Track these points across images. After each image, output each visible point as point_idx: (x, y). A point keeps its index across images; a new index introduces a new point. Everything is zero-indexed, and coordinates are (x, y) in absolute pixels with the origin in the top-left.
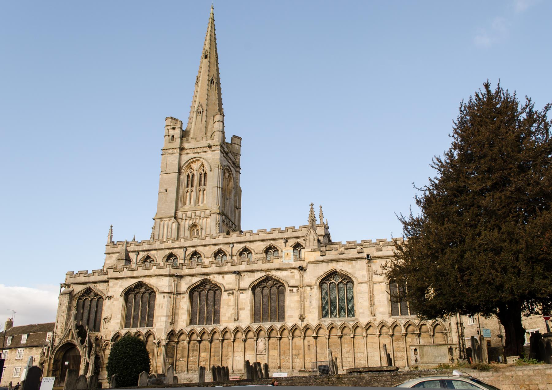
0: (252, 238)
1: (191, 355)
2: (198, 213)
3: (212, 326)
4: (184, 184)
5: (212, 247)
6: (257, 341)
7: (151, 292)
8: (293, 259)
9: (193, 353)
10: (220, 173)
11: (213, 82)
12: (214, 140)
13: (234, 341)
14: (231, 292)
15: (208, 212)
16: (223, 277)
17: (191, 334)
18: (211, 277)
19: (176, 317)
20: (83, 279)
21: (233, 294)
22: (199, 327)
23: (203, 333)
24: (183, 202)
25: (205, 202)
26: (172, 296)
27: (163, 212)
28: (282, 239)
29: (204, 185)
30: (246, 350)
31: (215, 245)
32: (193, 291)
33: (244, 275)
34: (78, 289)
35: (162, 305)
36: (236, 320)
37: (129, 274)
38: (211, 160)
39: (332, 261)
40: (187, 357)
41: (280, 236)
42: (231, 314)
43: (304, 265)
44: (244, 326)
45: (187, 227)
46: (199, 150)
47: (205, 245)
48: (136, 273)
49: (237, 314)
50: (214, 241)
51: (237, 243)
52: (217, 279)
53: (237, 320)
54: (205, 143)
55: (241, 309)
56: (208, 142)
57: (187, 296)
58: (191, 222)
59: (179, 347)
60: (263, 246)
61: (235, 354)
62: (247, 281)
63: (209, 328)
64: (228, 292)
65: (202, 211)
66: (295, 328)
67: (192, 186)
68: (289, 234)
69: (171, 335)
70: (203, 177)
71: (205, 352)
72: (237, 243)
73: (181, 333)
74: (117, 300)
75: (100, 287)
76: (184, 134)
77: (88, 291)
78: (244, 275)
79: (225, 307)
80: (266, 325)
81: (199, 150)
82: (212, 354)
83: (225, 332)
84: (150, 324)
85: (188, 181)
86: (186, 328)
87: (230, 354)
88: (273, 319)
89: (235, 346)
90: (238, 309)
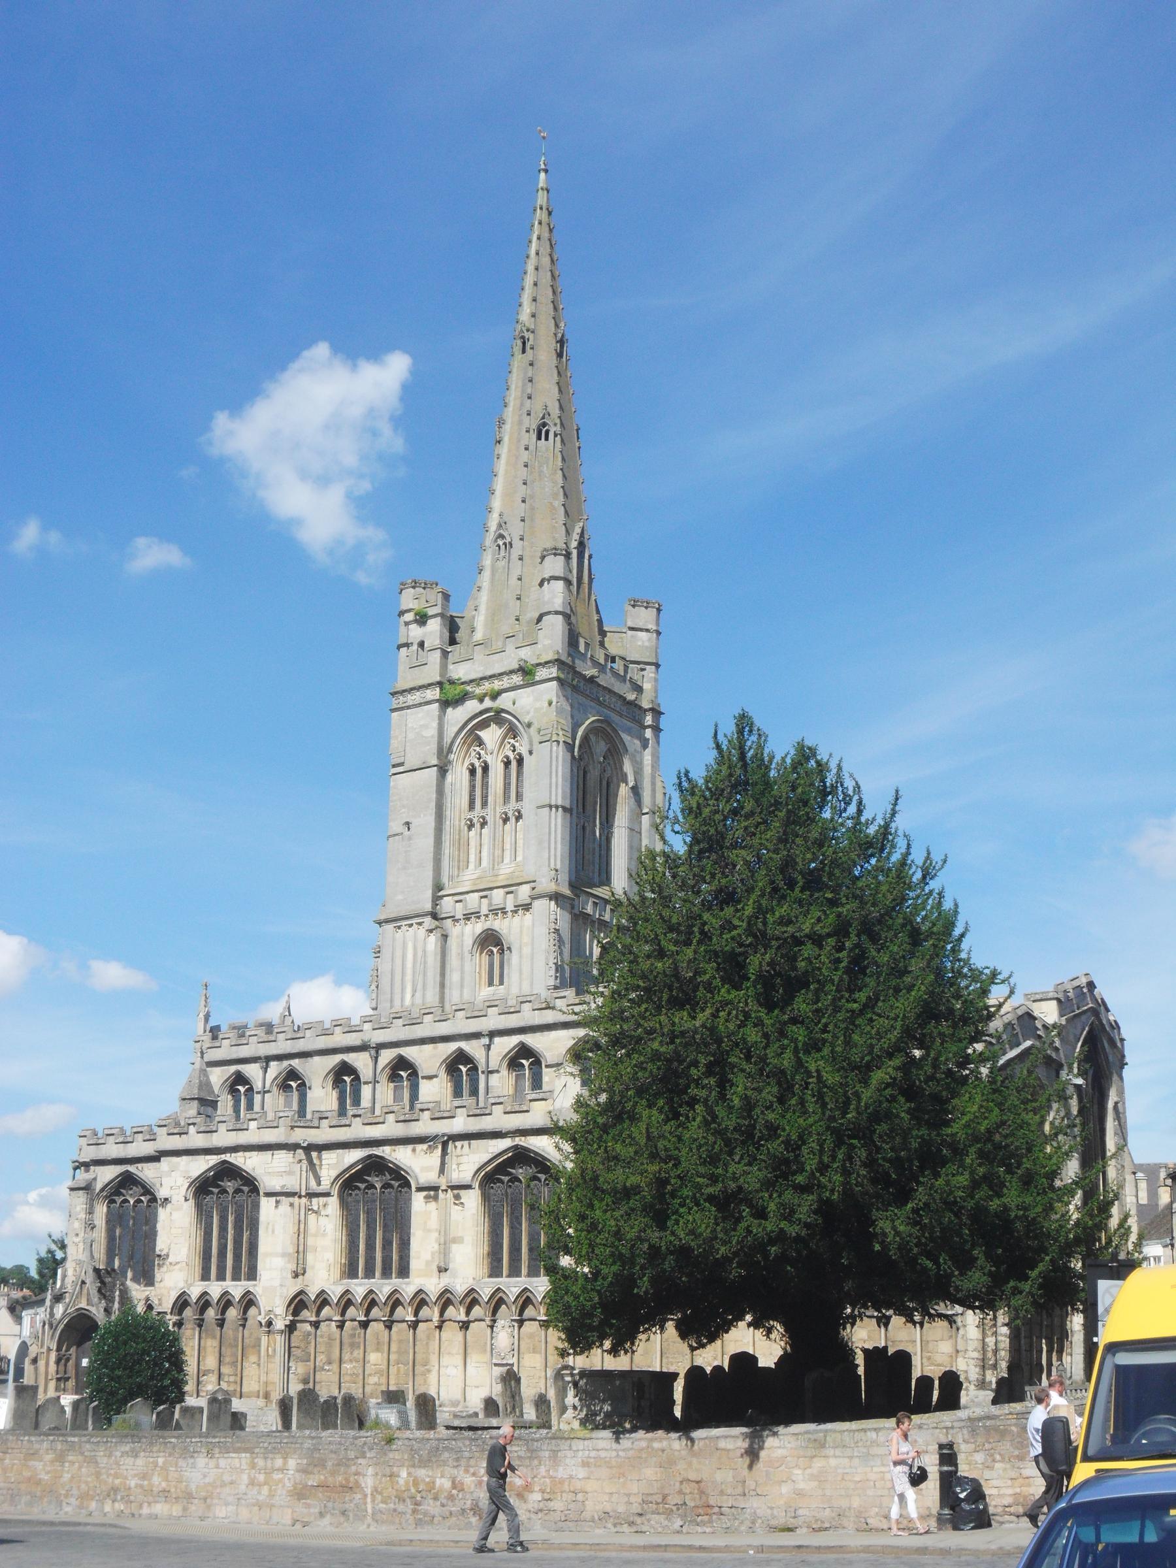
1: (346, 1357)
3: (389, 1284)
4: (458, 801)
5: (441, 1046)
6: (492, 1327)
9: (351, 1353)
10: (557, 757)
11: (547, 432)
12: (539, 646)
13: (440, 1327)
14: (432, 1193)
15: (524, 892)
16: (414, 1150)
17: (346, 1302)
18: (385, 1152)
19: (310, 1258)
20: (112, 1150)
21: (436, 1198)
22: (361, 1285)
23: (371, 1302)
24: (459, 861)
25: (519, 859)
26: (296, 1200)
27: (400, 897)
29: (517, 801)
30: (469, 1350)
33: (462, 1146)
34: (106, 1174)
35: (273, 1226)
36: (442, 1270)
37: (199, 1141)
38: (532, 714)
40: (338, 1362)
42: (433, 1254)
44: (460, 1288)
45: (469, 941)
46: (497, 685)
47: (423, 1041)
50: (444, 1029)
52: (401, 1156)
53: (446, 1270)
54: (510, 660)
55: (456, 1240)
58: (478, 927)
59: (322, 1336)
61: (445, 1360)
63: (383, 1288)
64: (424, 1193)
65: (509, 888)
67: (484, 804)
69: (298, 1304)
71: (378, 1350)
73: (323, 1300)
75: (146, 1172)
77: (127, 1181)
78: (462, 1146)
82: (393, 1357)
83: (420, 1300)
84: (252, 1275)
85: (472, 788)
86: (333, 1287)
87: (434, 1359)
89: (443, 1339)
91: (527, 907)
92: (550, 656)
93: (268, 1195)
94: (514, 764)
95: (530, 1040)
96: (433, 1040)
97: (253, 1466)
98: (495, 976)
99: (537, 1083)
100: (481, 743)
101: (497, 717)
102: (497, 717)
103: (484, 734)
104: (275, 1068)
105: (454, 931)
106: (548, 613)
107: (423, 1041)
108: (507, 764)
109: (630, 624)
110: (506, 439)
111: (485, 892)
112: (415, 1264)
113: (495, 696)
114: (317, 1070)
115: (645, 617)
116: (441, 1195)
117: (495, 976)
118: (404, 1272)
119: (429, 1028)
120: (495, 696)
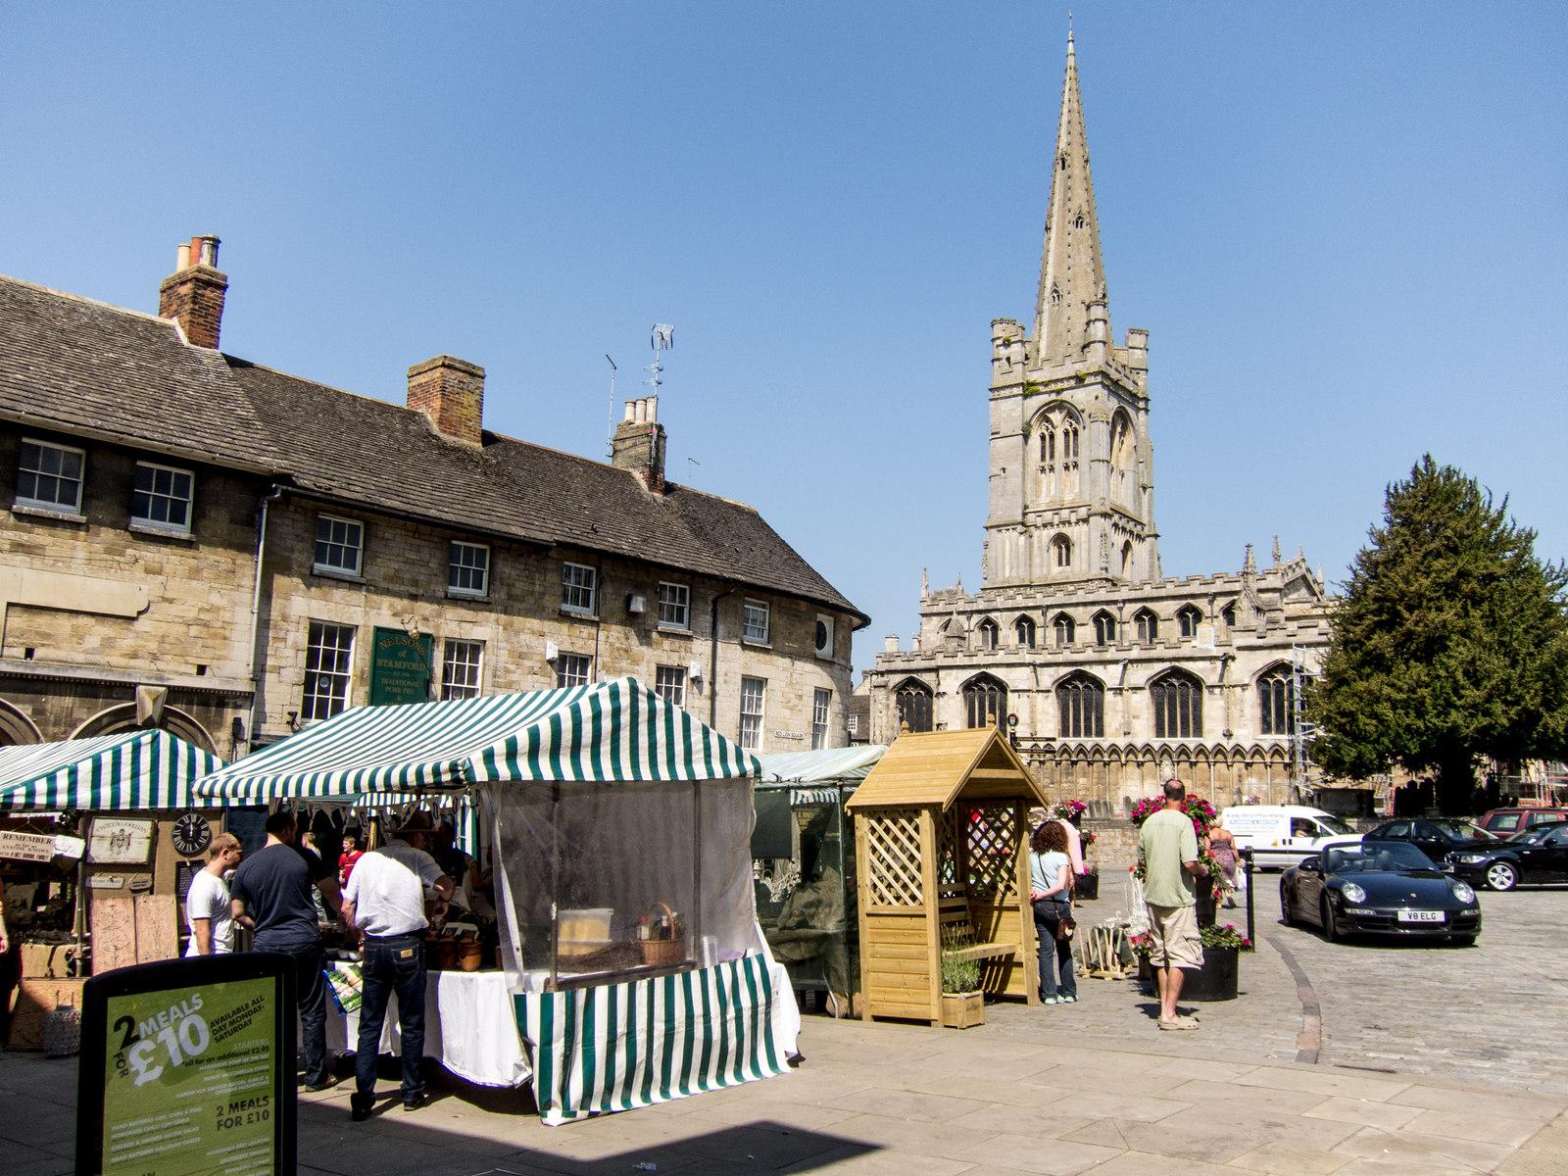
0: (1155, 593)
1: (1064, 780)
2: (1065, 514)
5: (1089, 608)
8: (1213, 643)
12: (1089, 362)
18: (1086, 668)
20: (899, 665)
21: (1121, 694)
28: (1206, 595)
31: (1093, 603)
32: (1062, 685)
34: (898, 678)
36: (1127, 734)
37: (966, 661)
39: (1276, 647)
41: (1204, 589)
43: (1232, 651)
44: (1139, 744)
46: (1060, 386)
47: (1077, 605)
48: (975, 661)
49: (1128, 724)
50: (1091, 598)
51: (1130, 601)
52: (1096, 671)
56: (1078, 366)
57: (1053, 695)
58: (1052, 532)
60: (1174, 606)
63: (1089, 742)
65: (1073, 509)
66: (1219, 750)
67: (1052, 457)
68: (1219, 586)
72: (1130, 601)
74: (953, 698)
75: (927, 678)
77: (911, 682)
79: (1110, 713)
80: (1174, 743)
81: (1060, 386)
83: (1114, 750)
85: (1043, 448)
88: (1185, 734)
90: (1130, 716)
91: (1086, 521)
92: (1095, 369)
93: (1013, 691)
94: (1071, 434)
95: (1149, 605)
96: (1085, 604)
97: (1124, 835)
98: (1065, 559)
99: (1154, 633)
100: (1048, 420)
101: (1060, 405)
102: (1060, 405)
103: (1051, 416)
104: (976, 618)
105: (1036, 533)
106: (1094, 342)
107: (1077, 605)
108: (1066, 434)
109: (1130, 345)
110: (1054, 227)
111: (1056, 511)
112: (1107, 730)
113: (1058, 392)
114: (1005, 621)
115: (1138, 340)
116: (1124, 692)
117: (1065, 559)
118: (1100, 733)
119: (1081, 597)
120: (1058, 392)
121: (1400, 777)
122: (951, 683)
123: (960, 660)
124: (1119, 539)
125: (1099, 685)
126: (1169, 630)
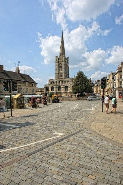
7: (54, 87)
54: (62, 60)
62: (64, 86)
63: (60, 91)
69: (56, 92)
70: (62, 66)
75: (48, 87)
76: (59, 59)
77: (47, 87)
80: (66, 91)
90: (63, 89)
117: (61, 76)
121: (78, 94)
122: (50, 87)
123: (51, 85)
124: (66, 75)
125: (61, 87)
126: (67, 83)
